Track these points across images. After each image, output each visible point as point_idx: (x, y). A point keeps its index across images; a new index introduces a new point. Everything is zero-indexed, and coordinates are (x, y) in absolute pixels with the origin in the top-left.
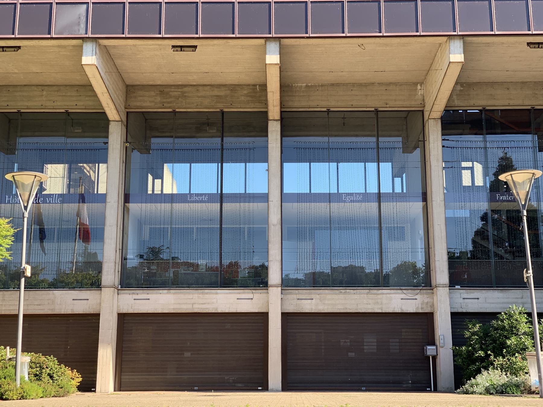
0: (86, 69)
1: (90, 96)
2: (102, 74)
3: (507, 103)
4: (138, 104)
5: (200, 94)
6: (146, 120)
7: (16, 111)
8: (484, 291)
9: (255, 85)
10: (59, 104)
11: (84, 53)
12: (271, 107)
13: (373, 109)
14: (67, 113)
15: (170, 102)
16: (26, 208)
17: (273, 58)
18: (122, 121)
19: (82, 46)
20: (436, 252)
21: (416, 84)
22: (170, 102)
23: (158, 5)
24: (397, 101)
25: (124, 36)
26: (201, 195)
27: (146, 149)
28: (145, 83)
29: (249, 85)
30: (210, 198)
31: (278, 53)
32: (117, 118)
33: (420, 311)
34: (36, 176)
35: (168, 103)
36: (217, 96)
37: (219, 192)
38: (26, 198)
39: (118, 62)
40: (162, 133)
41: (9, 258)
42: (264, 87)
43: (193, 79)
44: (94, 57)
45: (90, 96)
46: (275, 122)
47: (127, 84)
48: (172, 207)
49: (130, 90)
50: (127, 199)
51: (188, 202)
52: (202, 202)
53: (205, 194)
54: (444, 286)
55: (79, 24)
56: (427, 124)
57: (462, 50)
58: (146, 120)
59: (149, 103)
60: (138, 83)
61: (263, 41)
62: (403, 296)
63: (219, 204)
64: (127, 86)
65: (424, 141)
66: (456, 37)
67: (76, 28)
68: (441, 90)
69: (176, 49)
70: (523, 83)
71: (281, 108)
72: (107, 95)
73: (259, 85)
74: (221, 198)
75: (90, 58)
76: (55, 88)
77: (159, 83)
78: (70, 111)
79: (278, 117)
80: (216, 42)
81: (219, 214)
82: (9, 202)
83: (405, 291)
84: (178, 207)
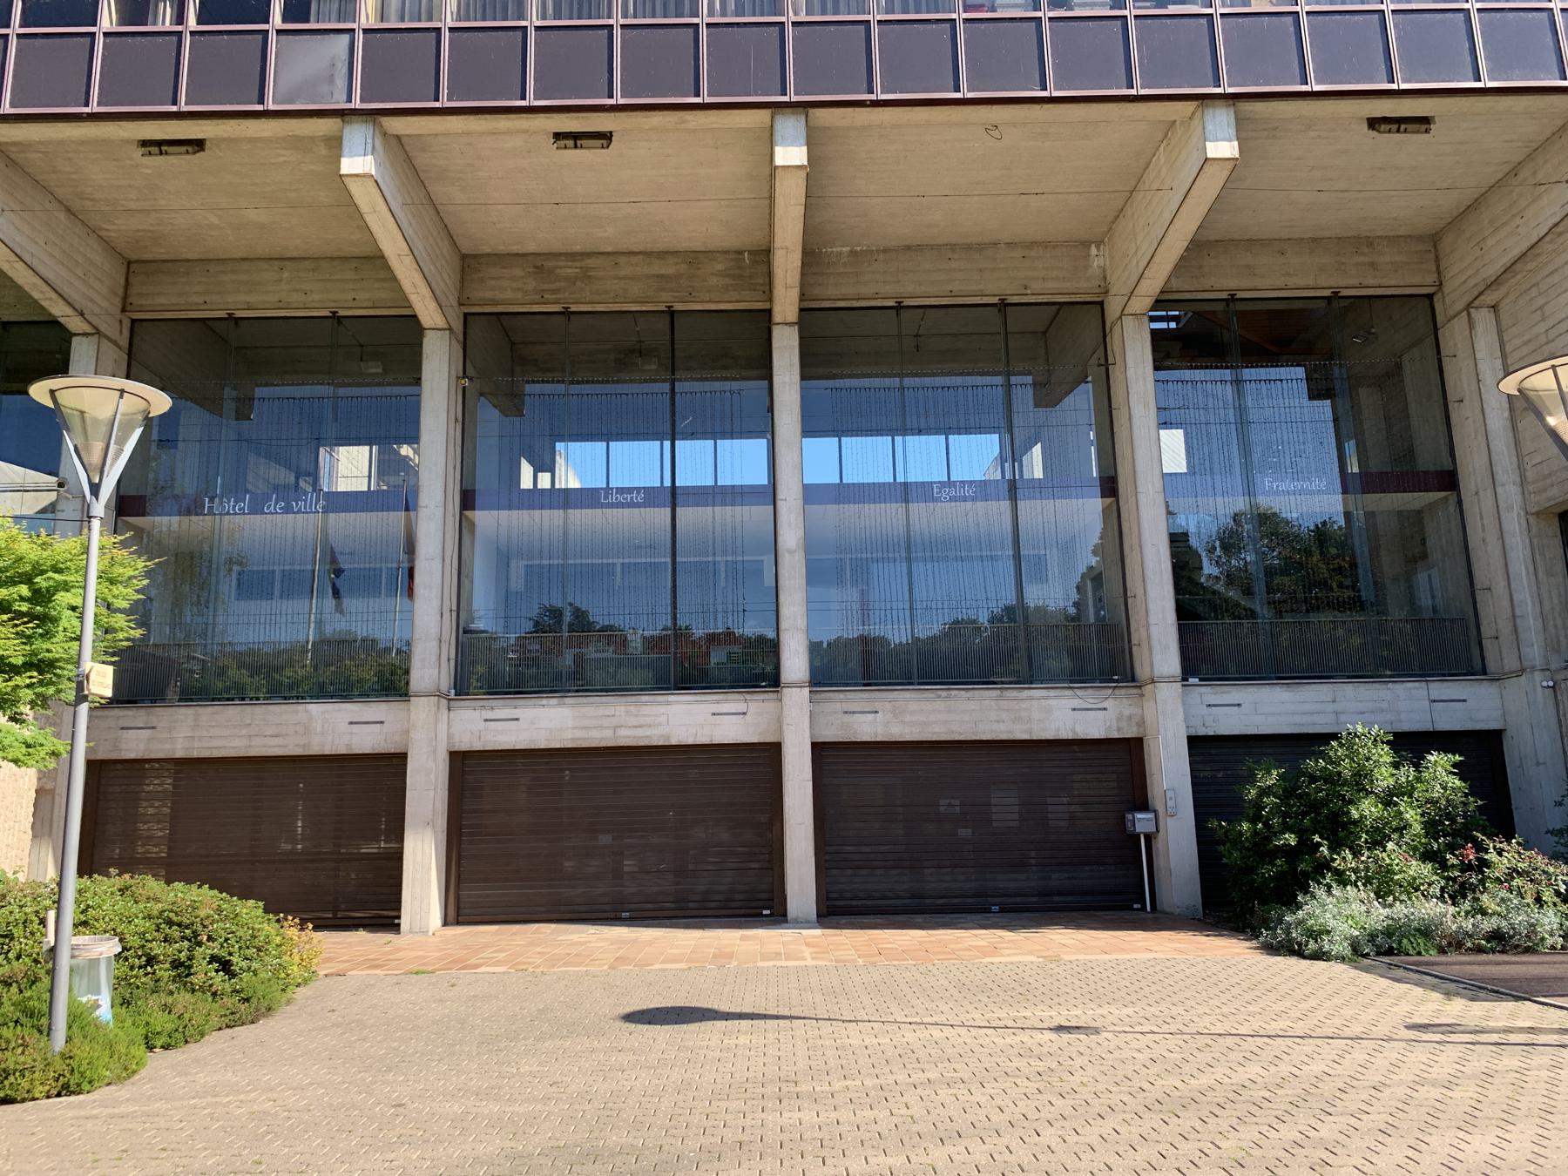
0: (354, 188)
1: (383, 280)
2: (409, 232)
3: (1280, 284)
4: (489, 295)
5: (622, 273)
6: (513, 344)
7: (222, 314)
8: (1251, 689)
9: (740, 252)
10: (317, 297)
11: (346, 150)
13: (995, 300)
16: (95, 489)
18: (450, 329)
20: (1151, 606)
21: (1086, 244)
23: (519, 34)
24: (1046, 281)
25: (438, 105)
26: (630, 490)
27: (512, 403)
28: (502, 249)
29: (726, 252)
30: (650, 497)
31: (803, 140)
32: (441, 323)
33: (1116, 735)
34: (122, 391)
36: (658, 276)
37: (667, 483)
38: (95, 457)
39: (437, 191)
40: (547, 369)
42: (764, 255)
43: (607, 236)
44: (370, 158)
48: (566, 518)
49: (470, 264)
50: (468, 500)
51: (602, 506)
52: (631, 505)
53: (638, 489)
54: (1169, 680)
55: (331, 79)
56: (1117, 329)
57: (1232, 132)
58: (513, 344)
59: (509, 293)
60: (486, 249)
61: (765, 114)
62: (1077, 703)
63: (668, 510)
64: (464, 257)
65: (1106, 365)
66: (1217, 102)
68: (1166, 239)
69: (562, 143)
70: (1314, 240)
71: (801, 300)
72: (409, 260)
74: (674, 496)
77: (532, 248)
78: (342, 313)
79: (792, 315)
80: (657, 118)
81: (669, 535)
82: (211, 512)
83: (1080, 693)
84: (580, 517)
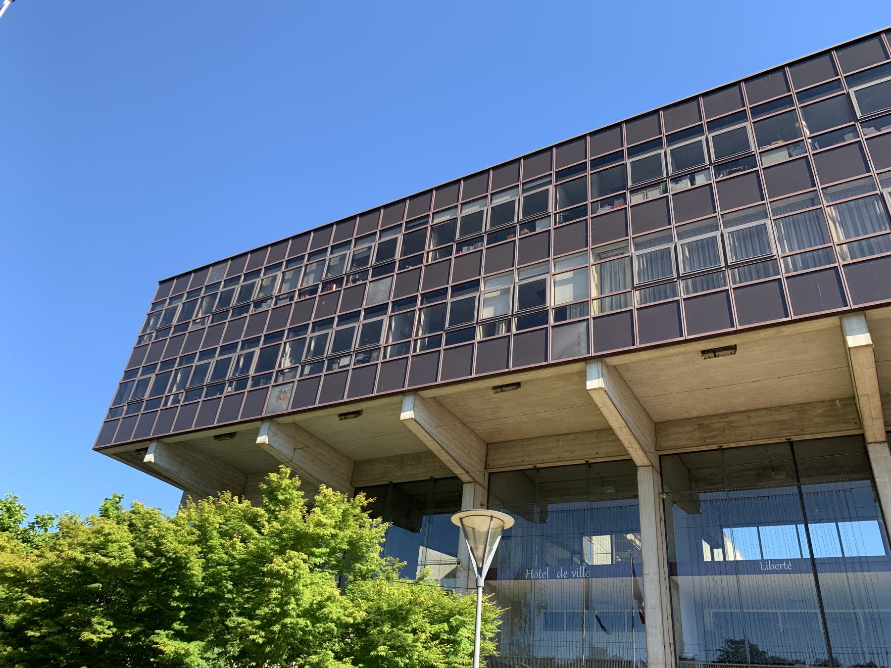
0: (594, 395)
1: (612, 441)
4: (672, 443)
5: (753, 422)
6: (689, 470)
7: (531, 467)
9: (833, 401)
10: (577, 454)
11: (588, 377)
12: (867, 422)
14: (588, 464)
15: (714, 437)
16: (480, 571)
17: (859, 339)
18: (652, 465)
19: (585, 372)
22: (714, 437)
23: (675, 305)
25: (634, 347)
26: (780, 561)
27: (693, 506)
28: (677, 417)
29: (823, 402)
30: (796, 566)
31: (866, 330)
32: (646, 462)
34: (492, 517)
35: (711, 438)
36: (779, 421)
37: (807, 555)
38: (480, 553)
39: (638, 390)
40: (711, 484)
41: (495, 653)
42: (851, 401)
43: (740, 402)
44: (601, 379)
45: (612, 441)
46: (879, 446)
47: (656, 418)
48: (738, 582)
49: (660, 428)
50: (672, 569)
51: (762, 573)
52: (783, 571)
53: (787, 561)
55: (579, 344)
58: (689, 470)
59: (685, 441)
60: (668, 418)
61: (835, 320)
63: (812, 575)
64: (656, 424)
67: (576, 349)
69: (707, 356)
71: (885, 426)
72: (626, 430)
73: (840, 400)
74: (814, 565)
75: (595, 383)
76: (571, 436)
77: (695, 414)
78: (591, 461)
79: (882, 436)
80: (763, 333)
82: (529, 578)
84: (748, 580)
